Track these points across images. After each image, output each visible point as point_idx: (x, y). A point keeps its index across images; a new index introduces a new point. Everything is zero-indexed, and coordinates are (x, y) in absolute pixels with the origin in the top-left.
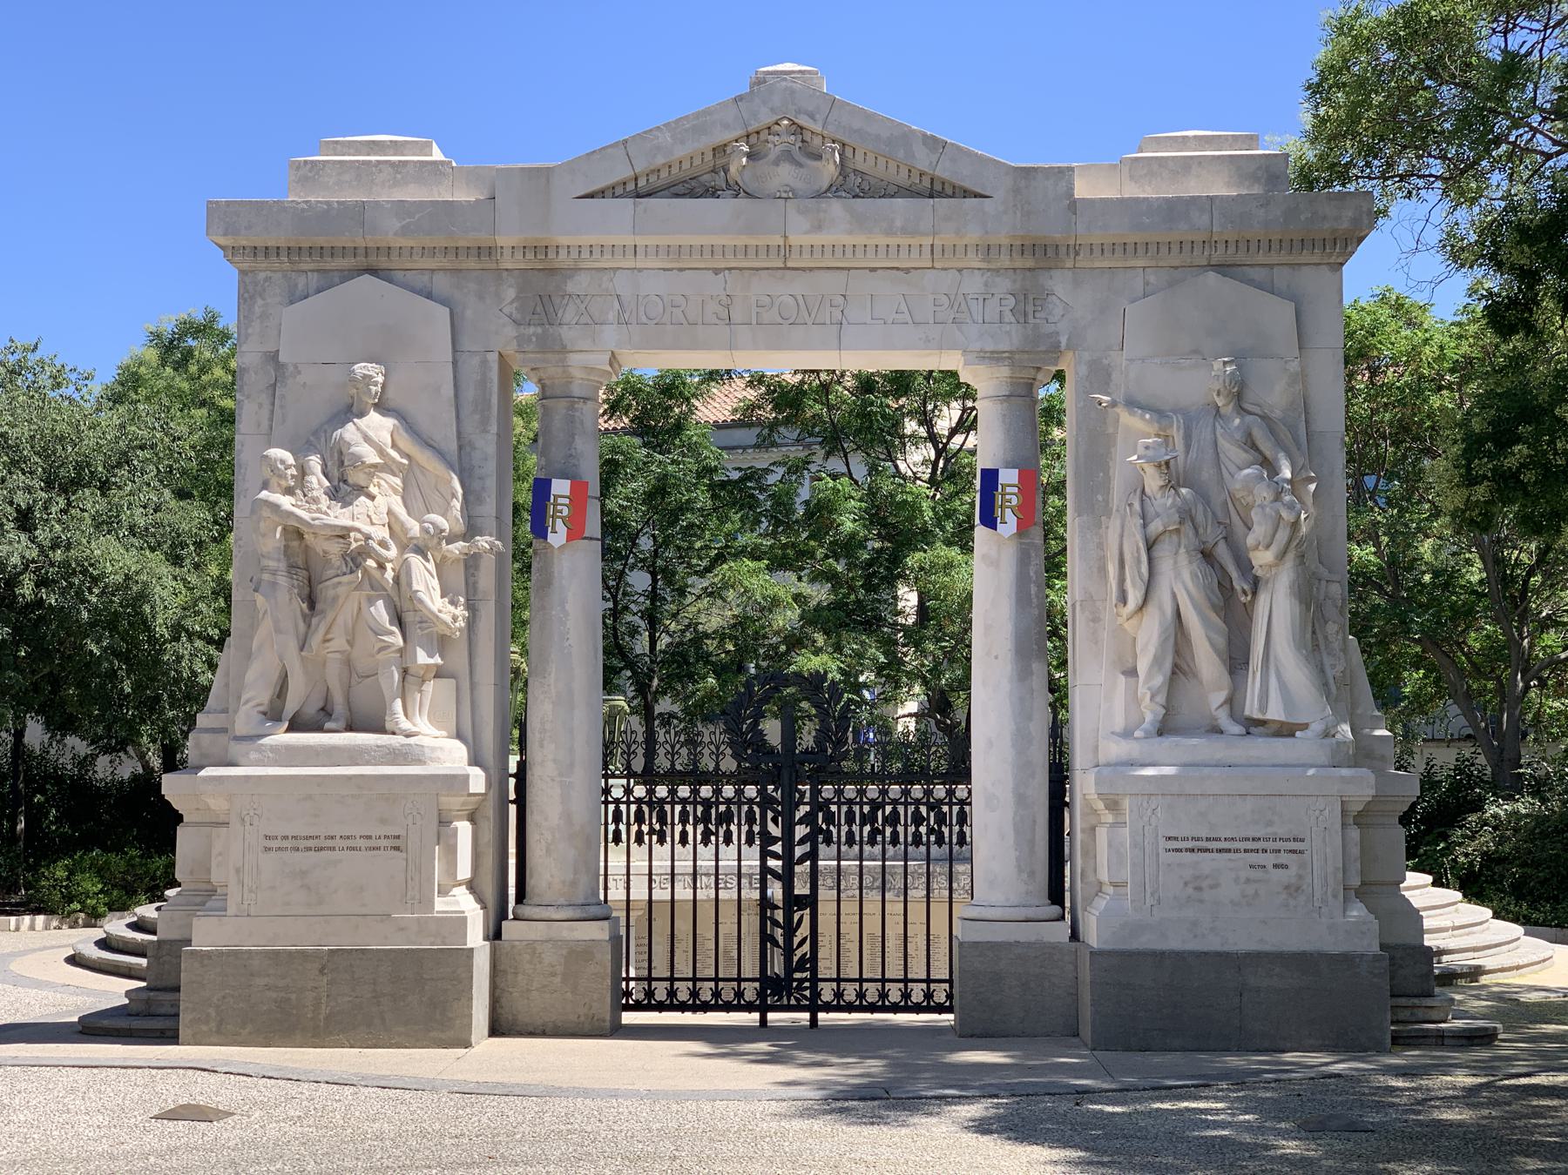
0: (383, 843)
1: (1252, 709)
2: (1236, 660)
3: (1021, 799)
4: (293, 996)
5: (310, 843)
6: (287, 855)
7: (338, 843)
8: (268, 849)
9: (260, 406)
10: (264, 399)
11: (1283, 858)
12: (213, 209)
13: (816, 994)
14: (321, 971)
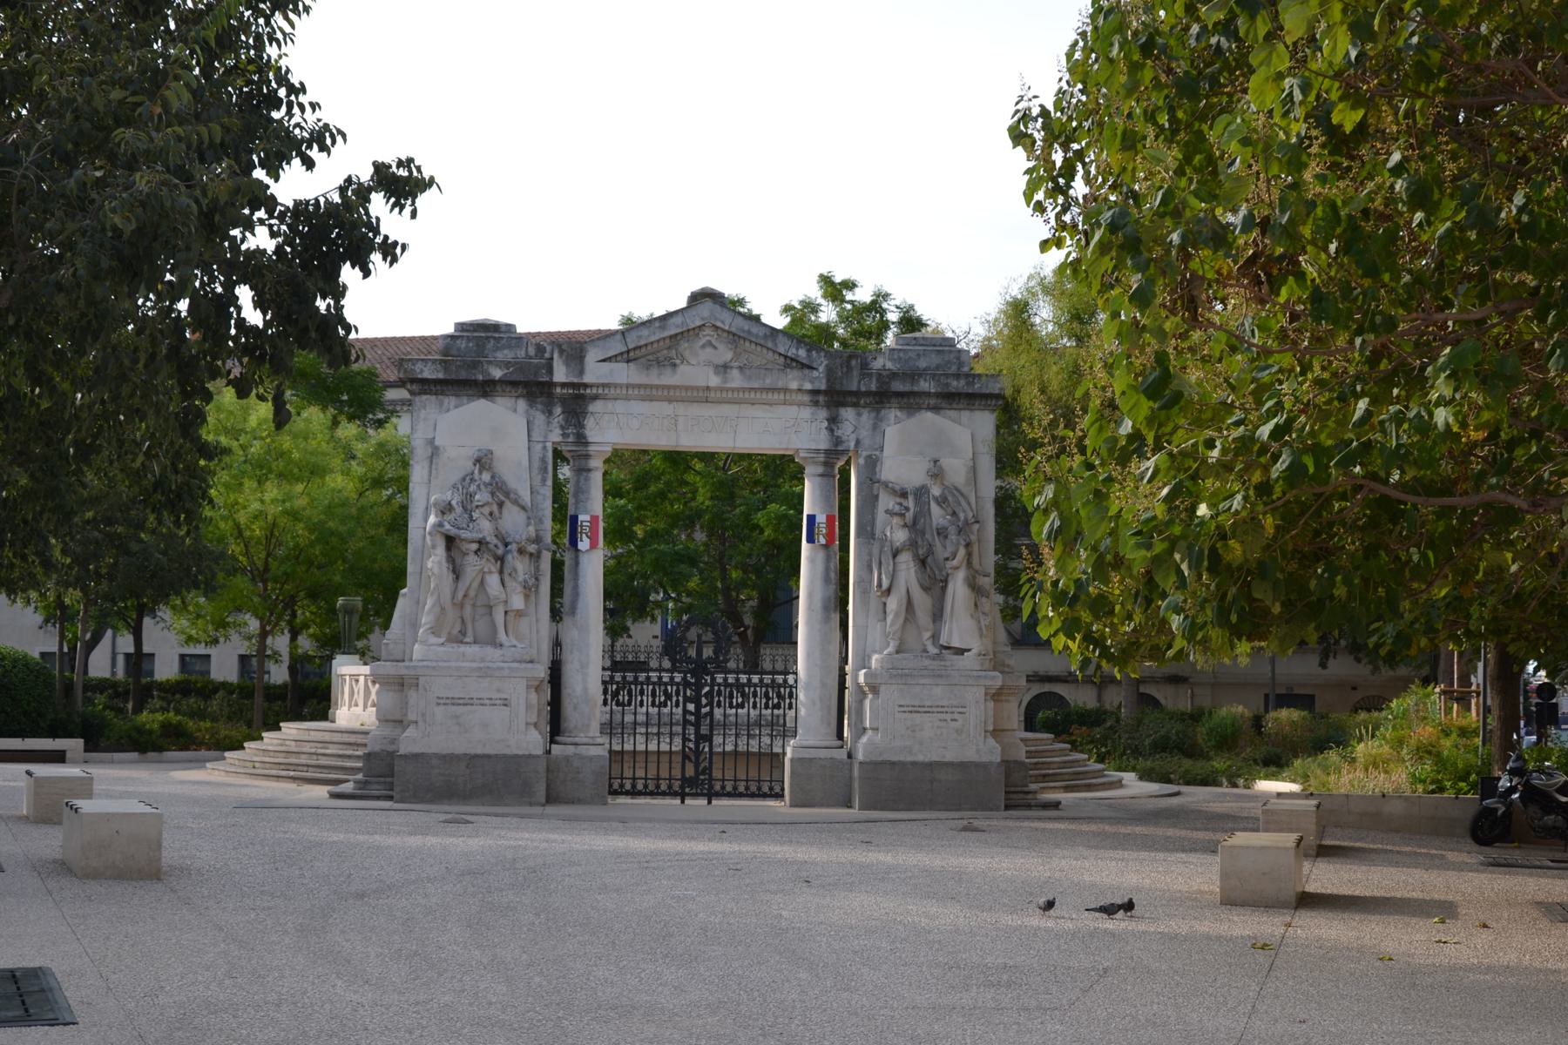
1: (943, 641)
2: (938, 615)
3: (823, 685)
10: (426, 464)
11: (956, 716)
13: (711, 787)
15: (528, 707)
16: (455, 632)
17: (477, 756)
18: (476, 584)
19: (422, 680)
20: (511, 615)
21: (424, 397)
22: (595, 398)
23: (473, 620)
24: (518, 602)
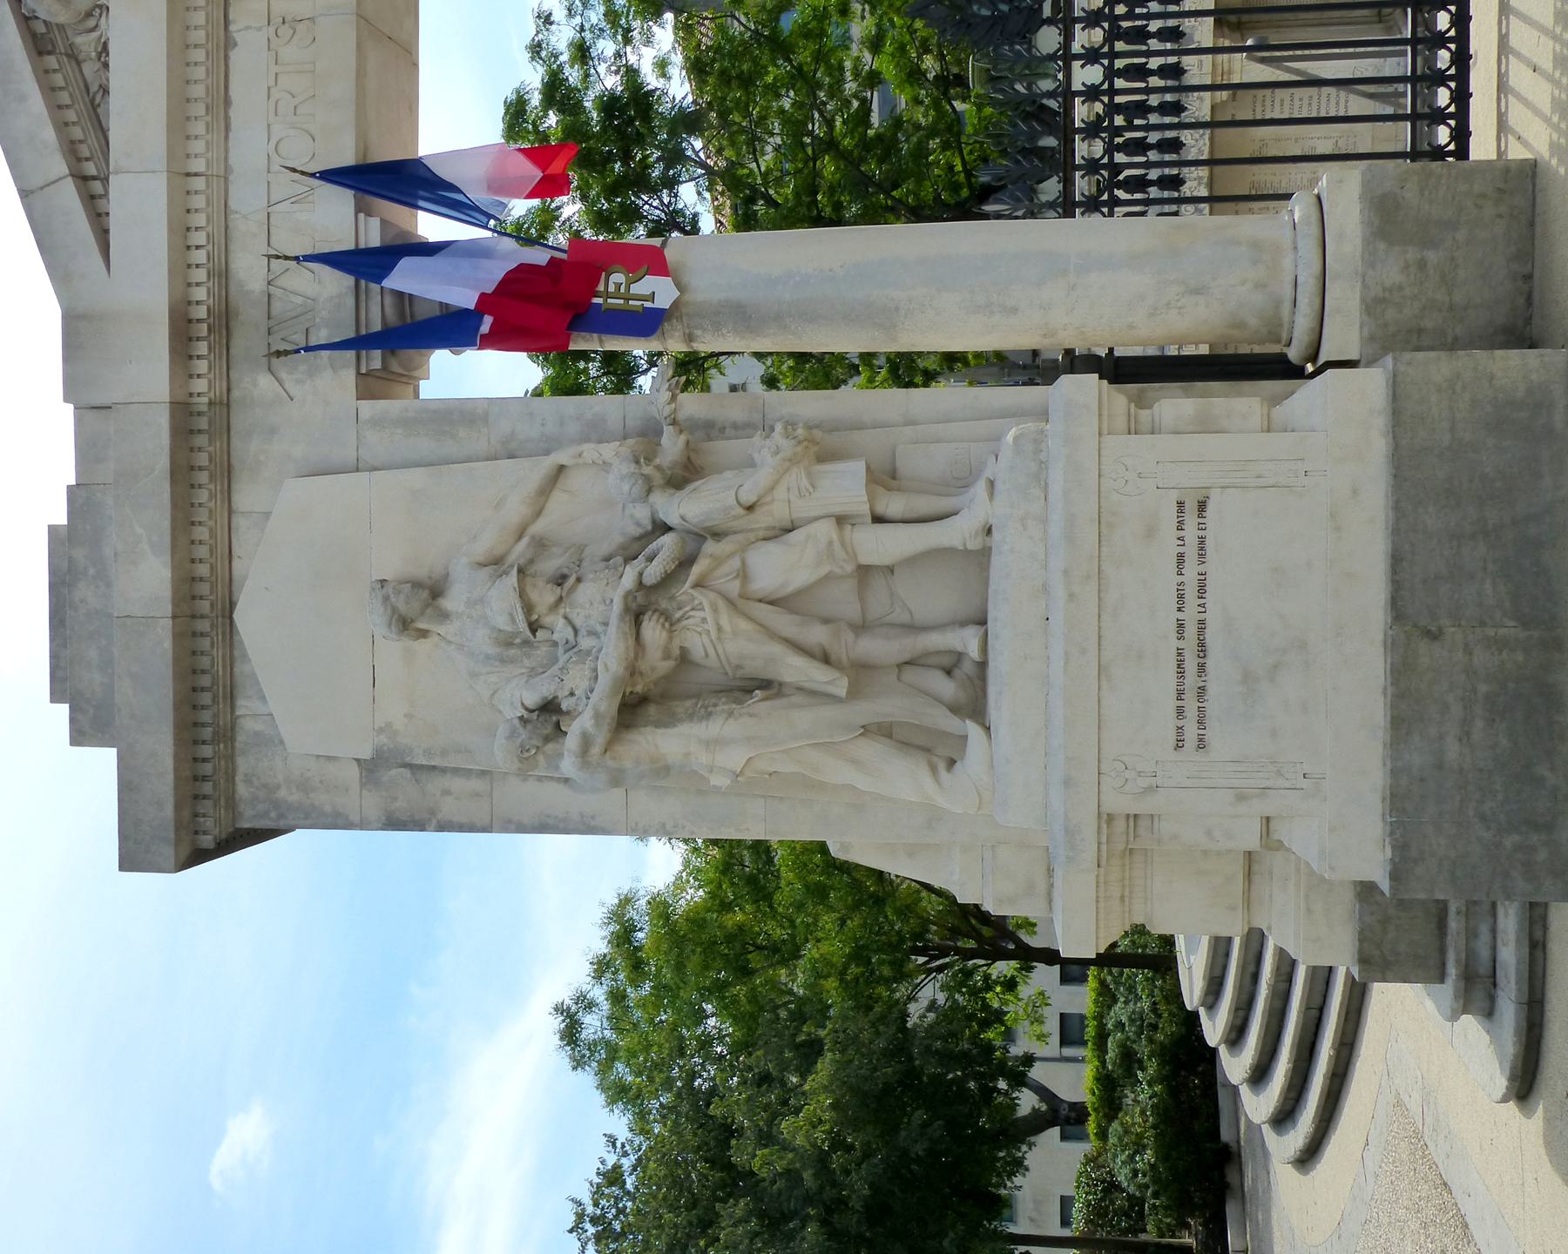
0: (1191, 533)
4: (1483, 688)
5: (1191, 665)
6: (1212, 708)
7: (1191, 615)
8: (1202, 744)
9: (447, 792)
10: (435, 785)
12: (130, 860)
14: (1434, 636)
15: (1205, 426)
16: (947, 688)
17: (1398, 609)
19: (1117, 803)
20: (893, 505)
21: (242, 790)
22: (222, 275)
23: (913, 628)
24: (845, 485)
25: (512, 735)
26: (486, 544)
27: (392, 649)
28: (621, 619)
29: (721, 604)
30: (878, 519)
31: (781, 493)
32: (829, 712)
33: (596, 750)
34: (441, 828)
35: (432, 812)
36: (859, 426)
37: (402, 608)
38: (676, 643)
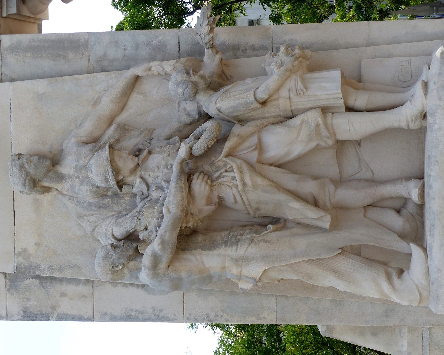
9: (63, 295)
10: (55, 290)
16: (397, 222)
18: (288, 180)
20: (360, 100)
23: (373, 182)
24: (328, 87)
25: (107, 256)
26: (87, 129)
27: (26, 200)
28: (179, 177)
29: (245, 168)
30: (350, 109)
31: (284, 93)
32: (317, 239)
33: (162, 266)
34: (60, 318)
35: (54, 308)
36: (336, 47)
37: (32, 171)
38: (216, 193)
